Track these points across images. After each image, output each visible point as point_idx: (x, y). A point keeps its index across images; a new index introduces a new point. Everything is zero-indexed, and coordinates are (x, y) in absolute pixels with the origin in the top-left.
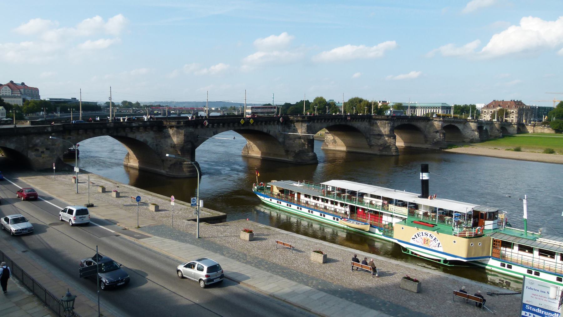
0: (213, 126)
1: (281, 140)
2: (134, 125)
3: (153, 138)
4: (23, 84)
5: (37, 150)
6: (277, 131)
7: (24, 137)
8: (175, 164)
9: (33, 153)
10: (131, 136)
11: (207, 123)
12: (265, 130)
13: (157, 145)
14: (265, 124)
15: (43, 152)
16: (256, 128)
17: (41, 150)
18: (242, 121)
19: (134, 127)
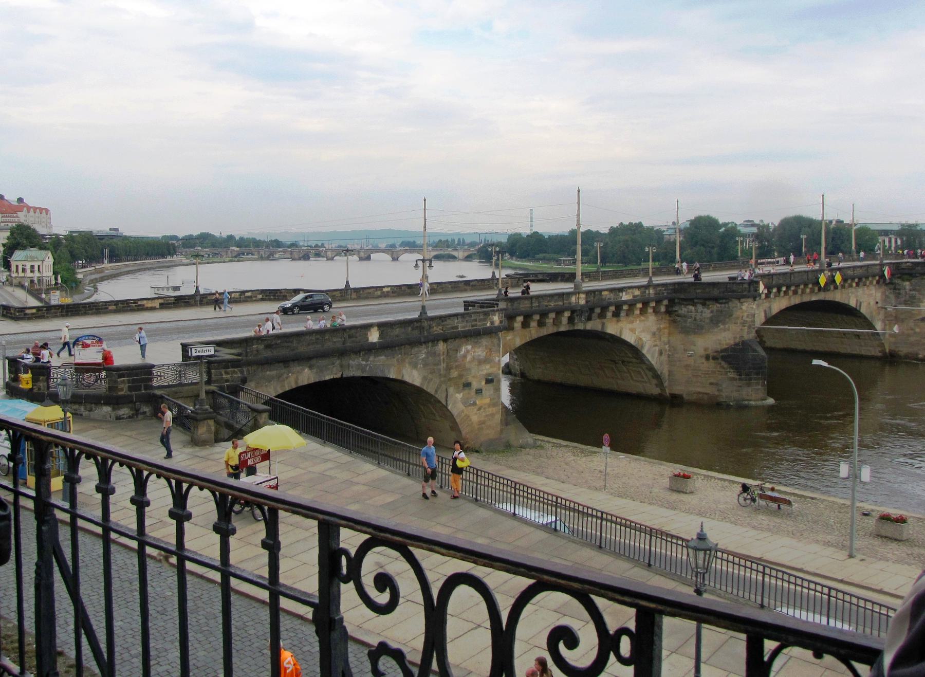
0: (767, 296)
1: (879, 326)
2: (625, 297)
3: (654, 334)
4: (20, 200)
5: (468, 385)
6: (872, 303)
7: (441, 346)
9: (459, 396)
10: (611, 328)
11: (762, 287)
12: (853, 303)
13: (661, 353)
14: (857, 285)
15: (479, 391)
16: (837, 296)
17: (475, 385)
18: (822, 280)
19: (625, 302)
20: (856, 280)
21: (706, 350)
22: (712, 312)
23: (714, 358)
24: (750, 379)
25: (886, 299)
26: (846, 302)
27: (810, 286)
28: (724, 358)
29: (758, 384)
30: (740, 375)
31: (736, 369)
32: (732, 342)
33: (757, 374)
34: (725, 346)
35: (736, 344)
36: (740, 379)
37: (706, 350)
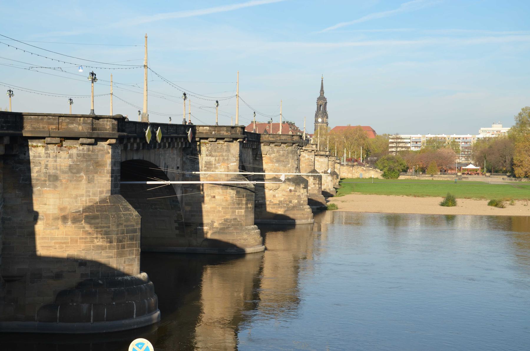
8: (80, 285)
14: (169, 146)
20: (170, 140)
21: (62, 209)
22: (71, 156)
23: (75, 220)
24: (123, 247)
25: (184, 163)
26: (158, 165)
27: (138, 140)
28: (89, 219)
29: (131, 253)
30: (111, 242)
31: (106, 233)
32: (97, 199)
33: (132, 239)
34: (89, 204)
35: (103, 201)
36: (110, 248)
37: (62, 209)
